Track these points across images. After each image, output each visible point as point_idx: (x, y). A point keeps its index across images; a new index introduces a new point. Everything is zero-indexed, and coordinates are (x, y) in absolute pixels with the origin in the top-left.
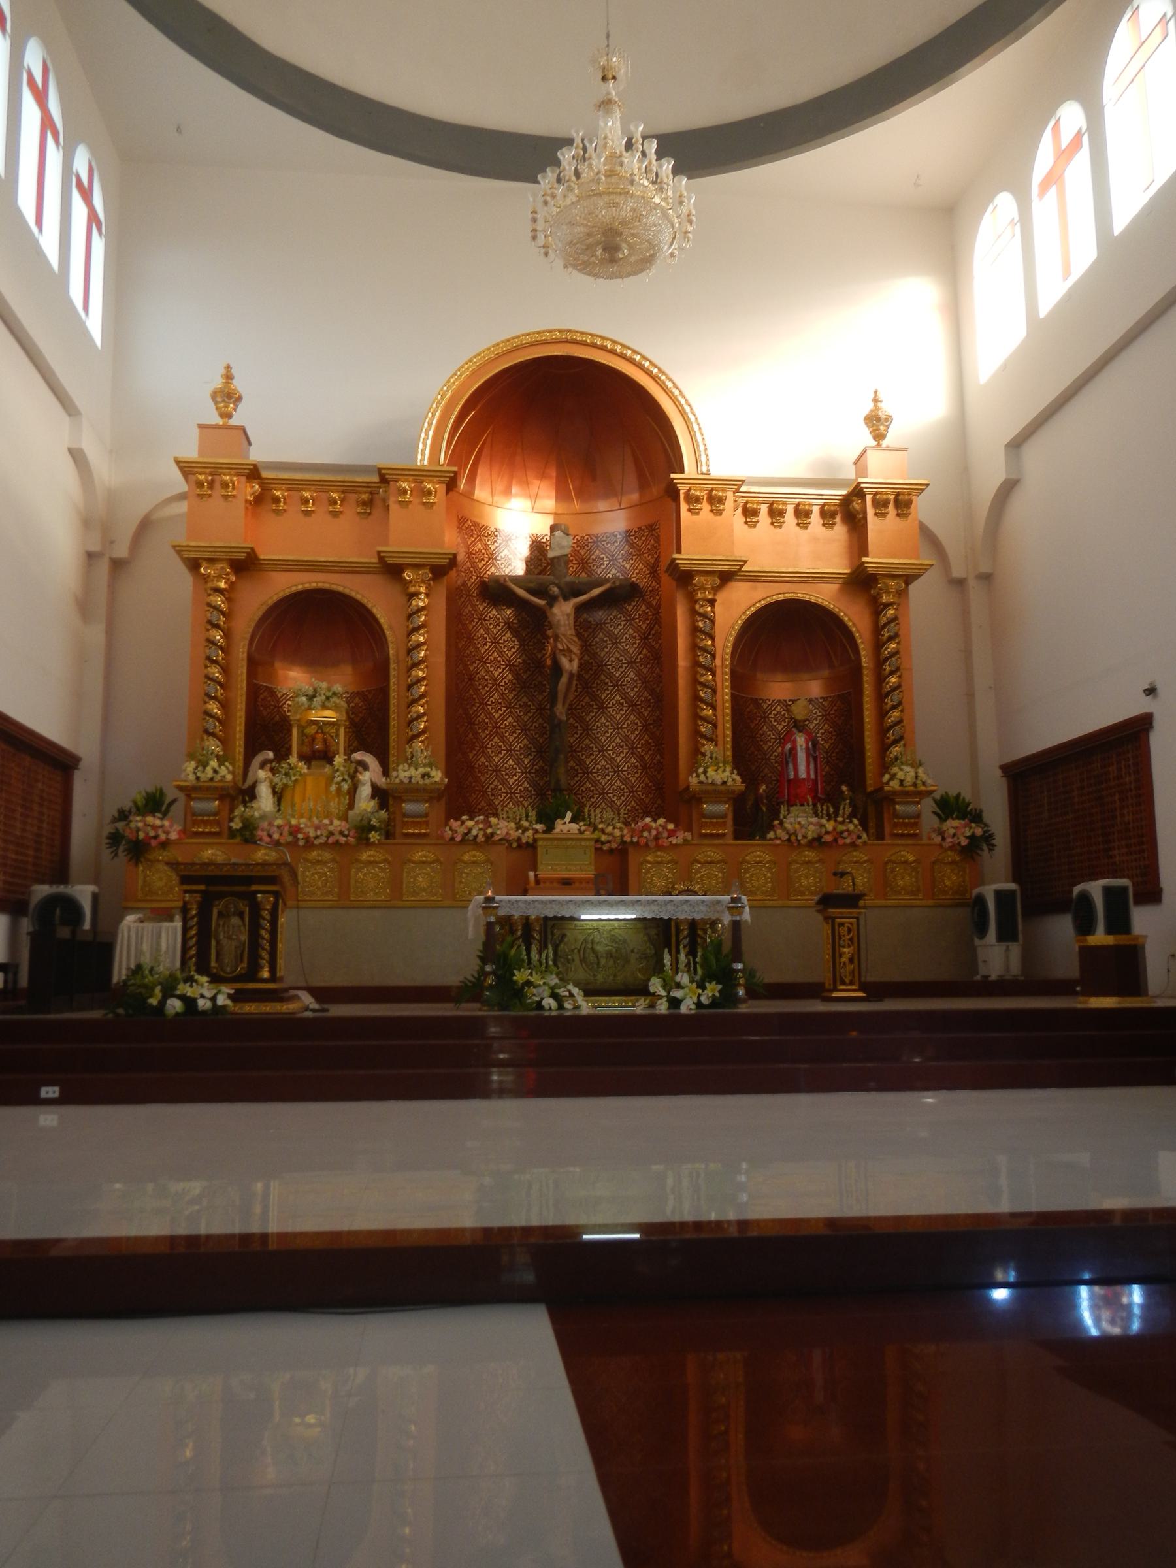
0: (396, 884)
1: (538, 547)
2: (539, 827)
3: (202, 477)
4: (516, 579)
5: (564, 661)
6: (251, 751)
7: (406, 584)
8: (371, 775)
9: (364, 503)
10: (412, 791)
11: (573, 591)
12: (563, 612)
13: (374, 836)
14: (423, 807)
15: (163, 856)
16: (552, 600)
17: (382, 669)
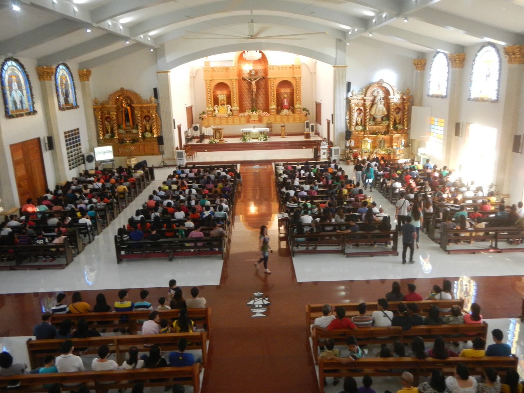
0: (233, 122)
1: (251, 71)
2: (251, 112)
3: (206, 69)
4: (246, 77)
5: (254, 90)
6: (214, 105)
7: (232, 81)
8: (230, 107)
9: (226, 70)
10: (235, 110)
11: (255, 79)
12: (254, 83)
13: (230, 116)
14: (236, 112)
15: (206, 119)
16: (252, 81)
17: (230, 91)
